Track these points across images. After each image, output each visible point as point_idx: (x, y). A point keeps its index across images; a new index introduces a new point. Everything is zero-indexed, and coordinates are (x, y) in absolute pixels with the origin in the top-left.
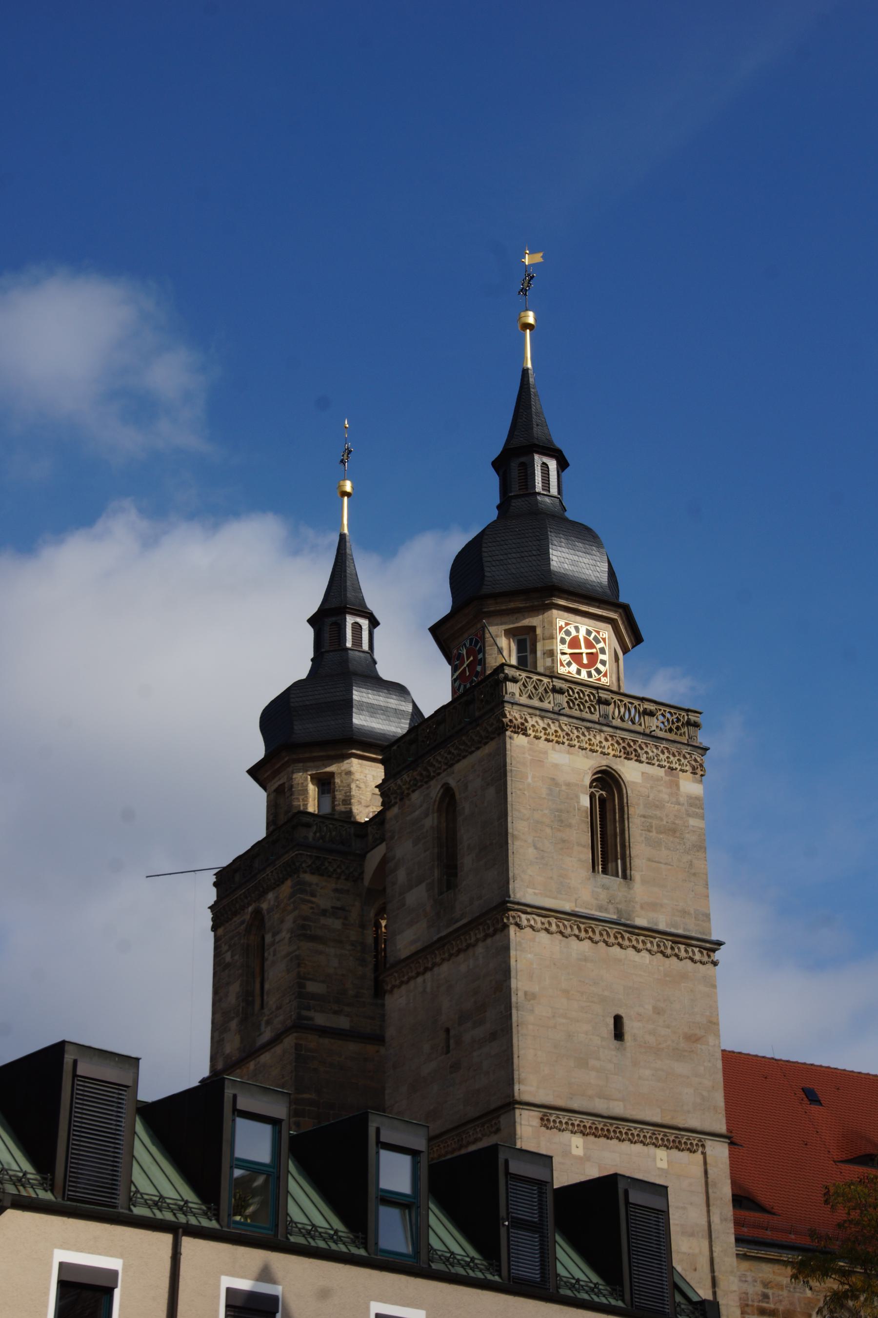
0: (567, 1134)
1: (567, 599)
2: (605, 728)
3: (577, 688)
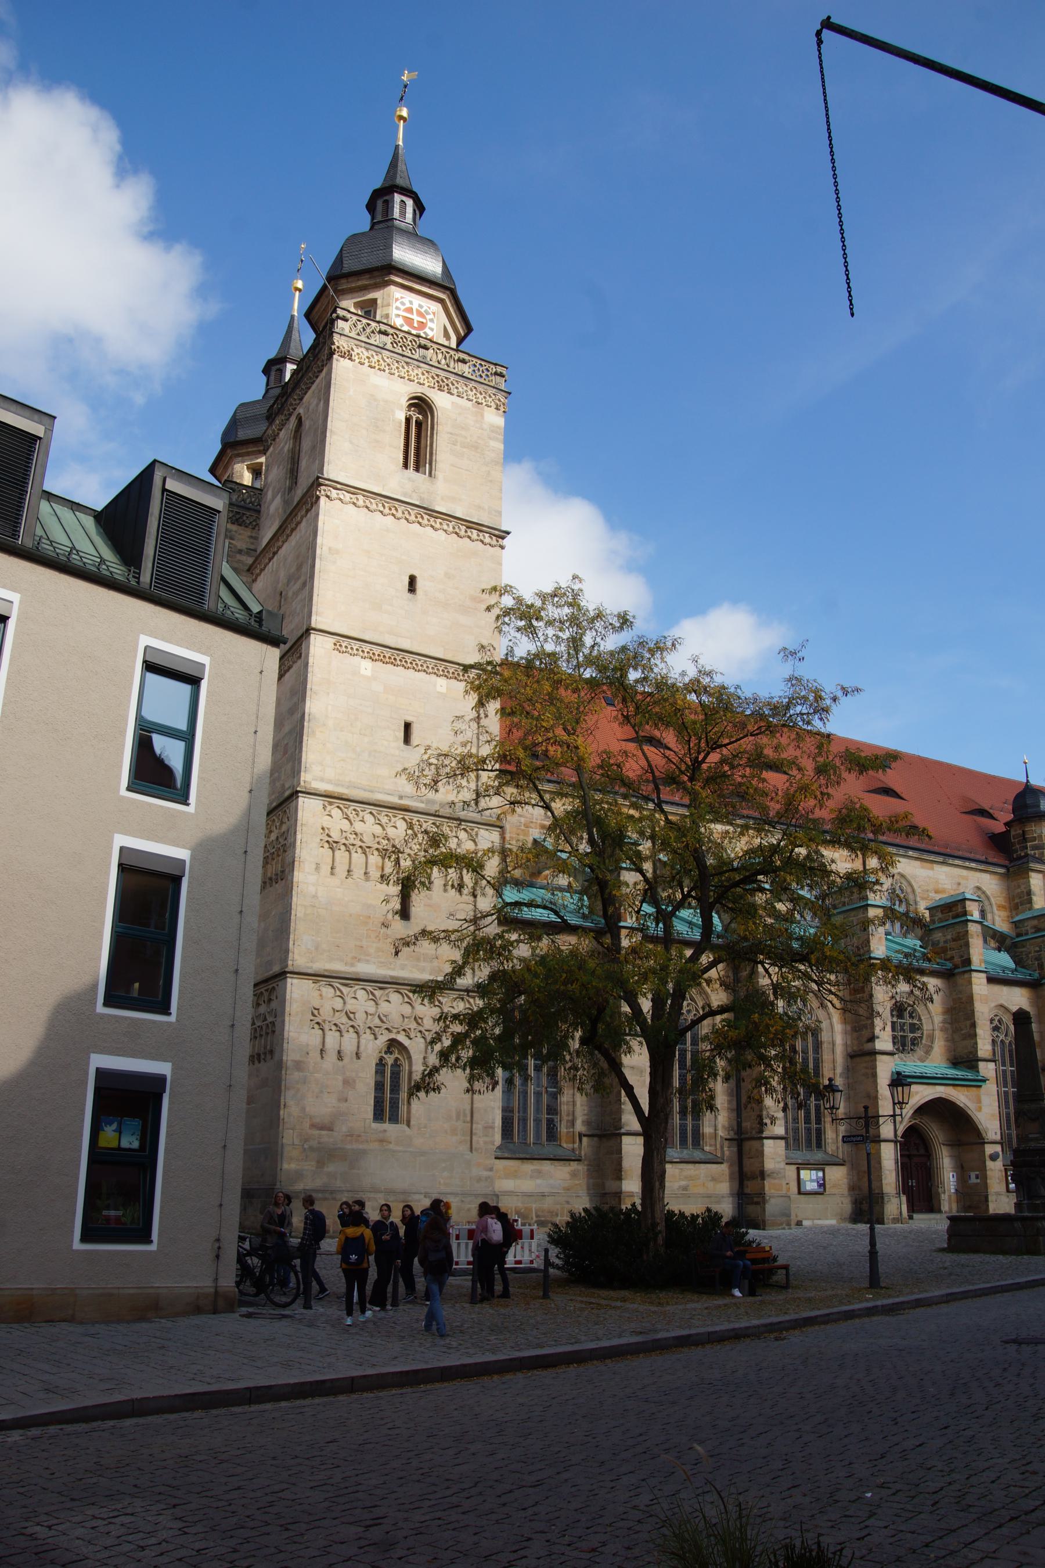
0: (357, 659)
1: (403, 278)
2: (422, 365)
3: (401, 335)
